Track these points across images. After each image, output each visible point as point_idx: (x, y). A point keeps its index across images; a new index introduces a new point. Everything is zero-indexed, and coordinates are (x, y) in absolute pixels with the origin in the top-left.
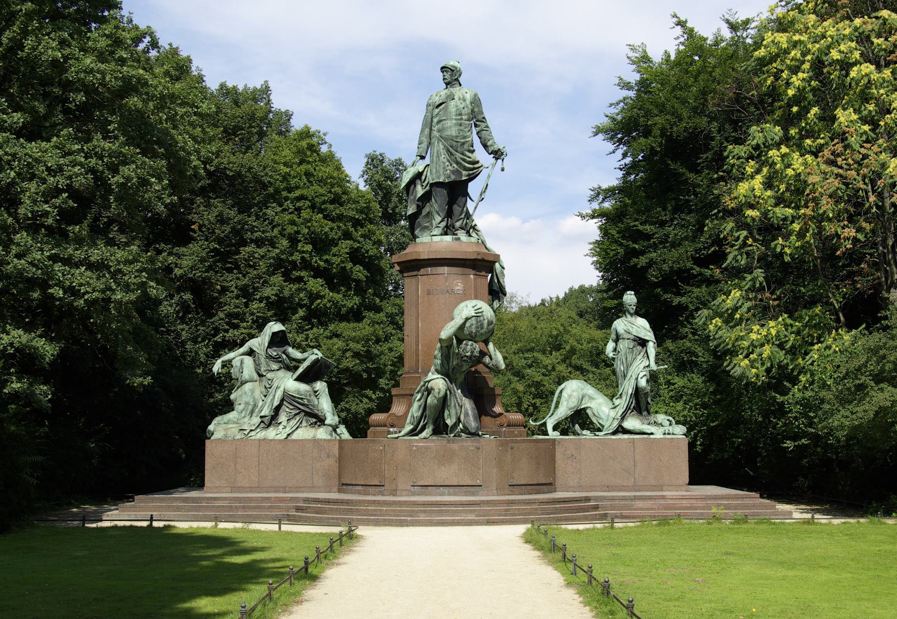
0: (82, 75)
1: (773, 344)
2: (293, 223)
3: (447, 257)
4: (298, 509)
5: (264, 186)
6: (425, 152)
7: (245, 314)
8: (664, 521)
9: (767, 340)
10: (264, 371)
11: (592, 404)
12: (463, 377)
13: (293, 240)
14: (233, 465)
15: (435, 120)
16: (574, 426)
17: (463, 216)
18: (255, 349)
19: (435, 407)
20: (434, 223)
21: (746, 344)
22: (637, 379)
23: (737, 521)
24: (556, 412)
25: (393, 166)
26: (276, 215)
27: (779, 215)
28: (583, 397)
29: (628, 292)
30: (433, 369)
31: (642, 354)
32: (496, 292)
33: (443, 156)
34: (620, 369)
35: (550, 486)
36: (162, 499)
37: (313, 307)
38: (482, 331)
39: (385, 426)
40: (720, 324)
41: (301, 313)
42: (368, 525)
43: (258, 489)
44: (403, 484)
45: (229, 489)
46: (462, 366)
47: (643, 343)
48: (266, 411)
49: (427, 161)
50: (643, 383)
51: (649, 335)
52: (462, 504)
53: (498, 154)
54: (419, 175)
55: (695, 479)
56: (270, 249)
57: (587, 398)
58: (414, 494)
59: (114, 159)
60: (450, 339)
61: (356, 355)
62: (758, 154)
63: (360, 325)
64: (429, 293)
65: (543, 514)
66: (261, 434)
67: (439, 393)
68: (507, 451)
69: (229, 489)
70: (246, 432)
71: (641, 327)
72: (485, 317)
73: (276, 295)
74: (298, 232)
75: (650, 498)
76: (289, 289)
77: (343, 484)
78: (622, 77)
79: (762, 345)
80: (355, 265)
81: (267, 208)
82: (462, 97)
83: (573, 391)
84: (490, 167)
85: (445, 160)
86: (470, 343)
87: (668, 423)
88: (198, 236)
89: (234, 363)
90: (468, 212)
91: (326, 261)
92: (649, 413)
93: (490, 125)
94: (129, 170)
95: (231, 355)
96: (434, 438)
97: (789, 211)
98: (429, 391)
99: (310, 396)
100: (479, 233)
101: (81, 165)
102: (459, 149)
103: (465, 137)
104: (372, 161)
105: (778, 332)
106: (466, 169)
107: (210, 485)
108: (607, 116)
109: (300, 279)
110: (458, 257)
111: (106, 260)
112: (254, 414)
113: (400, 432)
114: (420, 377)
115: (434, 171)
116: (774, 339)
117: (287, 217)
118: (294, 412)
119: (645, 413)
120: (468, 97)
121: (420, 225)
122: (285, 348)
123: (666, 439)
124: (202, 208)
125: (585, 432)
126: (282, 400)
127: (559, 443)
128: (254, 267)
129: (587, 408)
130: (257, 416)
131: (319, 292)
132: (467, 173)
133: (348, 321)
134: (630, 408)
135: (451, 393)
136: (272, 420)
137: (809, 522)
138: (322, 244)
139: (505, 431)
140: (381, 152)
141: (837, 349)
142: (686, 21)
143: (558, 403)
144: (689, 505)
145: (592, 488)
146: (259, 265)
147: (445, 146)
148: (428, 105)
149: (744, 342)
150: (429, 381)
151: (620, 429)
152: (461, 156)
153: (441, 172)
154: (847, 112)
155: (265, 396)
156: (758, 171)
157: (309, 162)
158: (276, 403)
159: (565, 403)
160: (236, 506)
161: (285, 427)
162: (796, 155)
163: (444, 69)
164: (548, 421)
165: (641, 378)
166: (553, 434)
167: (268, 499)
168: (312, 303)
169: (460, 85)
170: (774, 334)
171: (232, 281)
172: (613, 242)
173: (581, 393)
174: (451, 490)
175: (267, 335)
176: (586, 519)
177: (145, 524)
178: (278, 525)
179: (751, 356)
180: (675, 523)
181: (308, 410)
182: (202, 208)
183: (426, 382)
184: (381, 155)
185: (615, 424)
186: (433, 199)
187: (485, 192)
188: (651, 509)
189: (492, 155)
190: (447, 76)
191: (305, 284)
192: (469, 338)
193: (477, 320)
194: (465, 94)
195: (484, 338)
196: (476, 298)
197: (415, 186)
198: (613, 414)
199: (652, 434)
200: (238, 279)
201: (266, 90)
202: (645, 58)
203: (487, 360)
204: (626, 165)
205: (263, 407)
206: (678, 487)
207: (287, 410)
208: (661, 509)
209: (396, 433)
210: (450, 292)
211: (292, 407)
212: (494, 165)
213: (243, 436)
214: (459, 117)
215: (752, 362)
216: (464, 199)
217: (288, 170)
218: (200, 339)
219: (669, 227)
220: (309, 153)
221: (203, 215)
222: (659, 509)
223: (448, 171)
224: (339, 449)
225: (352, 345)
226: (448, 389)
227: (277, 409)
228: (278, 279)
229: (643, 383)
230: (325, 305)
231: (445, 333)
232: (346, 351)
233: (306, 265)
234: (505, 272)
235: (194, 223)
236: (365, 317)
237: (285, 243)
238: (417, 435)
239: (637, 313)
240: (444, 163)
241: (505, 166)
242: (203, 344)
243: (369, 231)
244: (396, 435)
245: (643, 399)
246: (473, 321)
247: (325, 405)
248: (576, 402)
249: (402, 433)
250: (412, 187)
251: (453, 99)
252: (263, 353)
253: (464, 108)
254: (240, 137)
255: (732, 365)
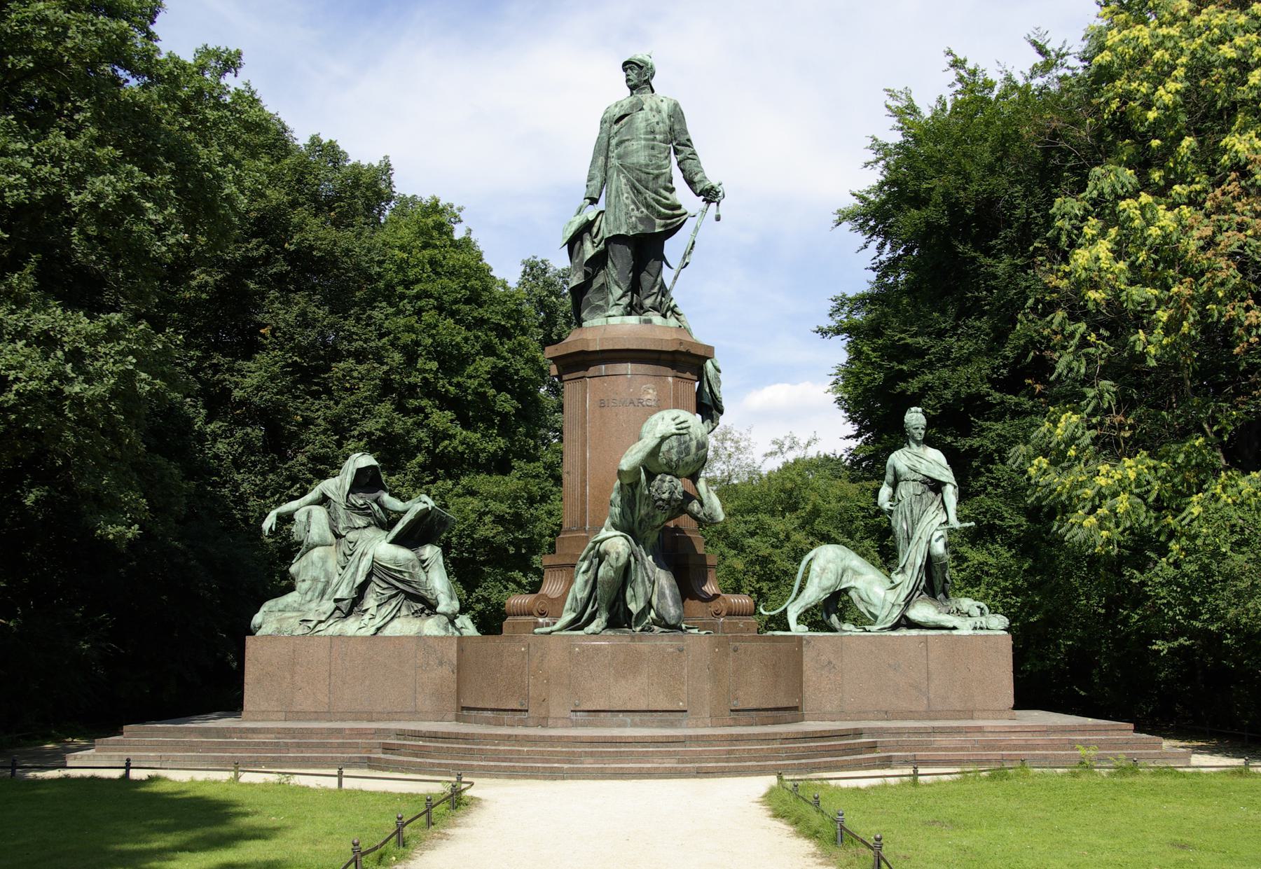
0: (29, 27)
1: (1131, 493)
2: (410, 329)
3: (631, 347)
4: (387, 748)
5: (370, 279)
6: (598, 192)
7: (337, 457)
8: (998, 775)
9: (1123, 486)
10: (344, 529)
11: (859, 583)
12: (656, 535)
13: (411, 356)
14: (289, 677)
15: (614, 142)
16: (829, 617)
17: (656, 290)
18: (330, 495)
19: (611, 582)
20: (611, 299)
21: (1089, 492)
22: (929, 542)
23: (1122, 771)
24: (802, 594)
25: (560, 277)
26: (386, 319)
27: (1135, 297)
28: (844, 571)
29: (913, 409)
30: (608, 522)
31: (936, 503)
32: (709, 408)
33: (626, 195)
34: (902, 527)
35: (793, 711)
36: (168, 731)
37: (437, 450)
38: (689, 459)
39: (530, 614)
40: (1045, 466)
41: (420, 458)
42: (497, 777)
43: (328, 715)
44: (558, 706)
45: (282, 715)
46: (654, 517)
47: (936, 486)
48: (344, 592)
49: (601, 205)
50: (939, 548)
51: (946, 475)
52: (655, 742)
53: (710, 195)
54: (587, 226)
55: (1024, 699)
56: (375, 365)
57: (849, 573)
58: (576, 725)
59: (77, 164)
60: (635, 471)
61: (499, 519)
62: (1104, 208)
63: (507, 478)
64: (602, 404)
65: (788, 758)
66: (335, 628)
67: (617, 559)
68: (727, 655)
69: (282, 715)
70: (311, 625)
71: (934, 462)
72: (693, 436)
73: (383, 430)
74: (417, 343)
75: (958, 731)
76: (401, 424)
77: (463, 708)
78: (877, 137)
79: (1115, 495)
80: (499, 391)
81: (373, 308)
82: (654, 107)
83: (829, 562)
84: (698, 215)
85: (628, 202)
86: (668, 478)
87: (978, 611)
88: (271, 343)
89: (296, 516)
90: (663, 286)
91: (458, 385)
92: (947, 597)
93: (697, 152)
94: (103, 182)
95: (293, 505)
96: (609, 633)
97: (1151, 292)
98: (601, 557)
99: (413, 567)
100: (681, 318)
101: (25, 173)
102: (650, 185)
103: (659, 167)
104: (532, 269)
105: (1139, 474)
106: (660, 216)
107: (251, 709)
108: (854, 195)
109: (420, 410)
110: (648, 348)
111: (60, 332)
112: (326, 597)
113: (554, 623)
114: (587, 537)
115: (612, 218)
116: (1133, 486)
117: (401, 321)
118: (389, 593)
119: (941, 596)
120: (665, 107)
121: (589, 303)
122: (378, 494)
123: (977, 636)
124: (277, 305)
125: (846, 626)
126: (370, 575)
127: (808, 642)
128: (351, 390)
129: (850, 588)
130: (330, 599)
131: (446, 429)
132: (662, 222)
133: (490, 473)
134: (917, 589)
135: (636, 560)
136: (353, 606)
137: (1241, 773)
138: (452, 361)
139: (723, 623)
140: (544, 258)
141: (1230, 501)
142: (965, 60)
143: (804, 580)
144: (1023, 743)
145: (861, 715)
146: (358, 389)
147: (628, 180)
148: (603, 122)
149: (1087, 490)
150: (601, 542)
151: (903, 622)
152: (654, 195)
153: (623, 219)
154: (1246, 137)
155: (343, 568)
156: (1103, 233)
157: (435, 247)
158: (360, 578)
159: (816, 581)
160: (286, 744)
161: (373, 617)
162: (1161, 209)
163: (627, 65)
164: (789, 609)
165: (937, 541)
166: (797, 629)
167: (339, 731)
168: (436, 445)
169: (653, 91)
170: (1132, 478)
171: (321, 411)
172: (868, 364)
173: (841, 565)
174: (637, 717)
175: (349, 473)
176: (858, 766)
177: (117, 774)
178: (337, 779)
179: (1099, 511)
180: (1018, 775)
181: (411, 590)
182: (277, 305)
183: (596, 543)
184: (543, 262)
185: (896, 613)
186: (610, 264)
187: (689, 253)
188: (962, 749)
189: (702, 197)
190: (633, 76)
191: (427, 417)
192: (667, 469)
193: (679, 441)
194: (660, 103)
195: (691, 470)
196: (676, 407)
197: (582, 244)
198: (891, 596)
199: (955, 628)
200: (328, 408)
201: (386, 168)
202: (912, 109)
203: (695, 506)
204: (881, 263)
205: (339, 584)
206: (997, 713)
207: (378, 589)
208: (978, 749)
209: (548, 625)
210: (637, 402)
211: (385, 586)
212: (704, 212)
213: (306, 631)
214: (651, 136)
215: (1101, 520)
216: (658, 263)
217: (405, 255)
218: (268, 494)
219: (951, 337)
220: (435, 233)
221: (278, 314)
222: (973, 748)
223: (634, 219)
224: (458, 651)
225: (493, 505)
226: (632, 553)
227: (362, 589)
228: (386, 408)
229: (939, 548)
230: (454, 448)
231: (626, 463)
232: (485, 513)
233: (429, 390)
234: (721, 376)
235: (265, 326)
236: (513, 468)
237: (398, 357)
238: (581, 628)
239: (929, 441)
240: (627, 205)
241: (721, 213)
242: (271, 500)
243: (520, 344)
244: (548, 629)
245: (939, 574)
246: (674, 442)
247: (438, 582)
248: (833, 578)
249: (558, 626)
250: (577, 245)
251: (642, 109)
252: (342, 501)
253: (658, 123)
254: (337, 210)
255: (1067, 526)
